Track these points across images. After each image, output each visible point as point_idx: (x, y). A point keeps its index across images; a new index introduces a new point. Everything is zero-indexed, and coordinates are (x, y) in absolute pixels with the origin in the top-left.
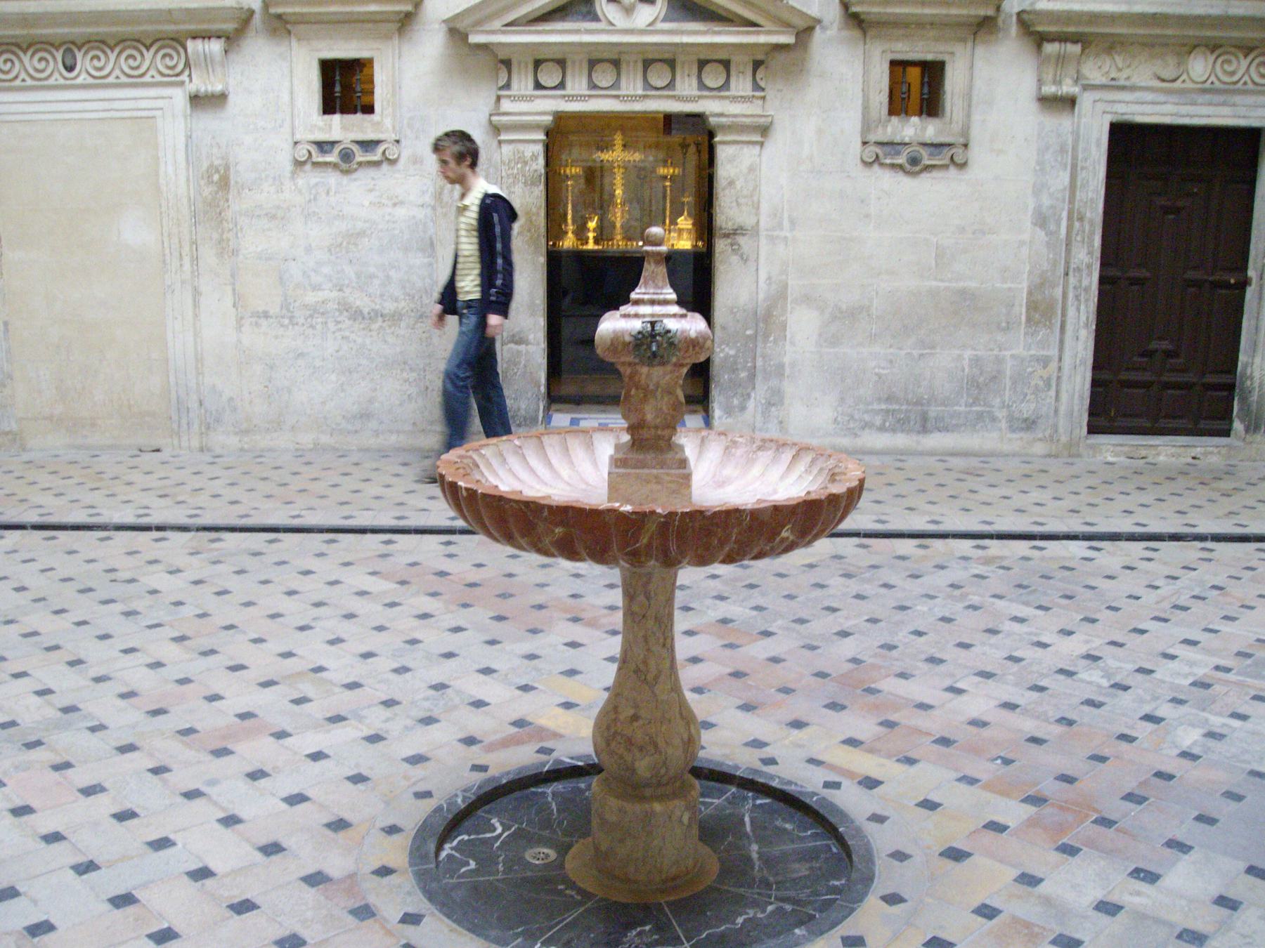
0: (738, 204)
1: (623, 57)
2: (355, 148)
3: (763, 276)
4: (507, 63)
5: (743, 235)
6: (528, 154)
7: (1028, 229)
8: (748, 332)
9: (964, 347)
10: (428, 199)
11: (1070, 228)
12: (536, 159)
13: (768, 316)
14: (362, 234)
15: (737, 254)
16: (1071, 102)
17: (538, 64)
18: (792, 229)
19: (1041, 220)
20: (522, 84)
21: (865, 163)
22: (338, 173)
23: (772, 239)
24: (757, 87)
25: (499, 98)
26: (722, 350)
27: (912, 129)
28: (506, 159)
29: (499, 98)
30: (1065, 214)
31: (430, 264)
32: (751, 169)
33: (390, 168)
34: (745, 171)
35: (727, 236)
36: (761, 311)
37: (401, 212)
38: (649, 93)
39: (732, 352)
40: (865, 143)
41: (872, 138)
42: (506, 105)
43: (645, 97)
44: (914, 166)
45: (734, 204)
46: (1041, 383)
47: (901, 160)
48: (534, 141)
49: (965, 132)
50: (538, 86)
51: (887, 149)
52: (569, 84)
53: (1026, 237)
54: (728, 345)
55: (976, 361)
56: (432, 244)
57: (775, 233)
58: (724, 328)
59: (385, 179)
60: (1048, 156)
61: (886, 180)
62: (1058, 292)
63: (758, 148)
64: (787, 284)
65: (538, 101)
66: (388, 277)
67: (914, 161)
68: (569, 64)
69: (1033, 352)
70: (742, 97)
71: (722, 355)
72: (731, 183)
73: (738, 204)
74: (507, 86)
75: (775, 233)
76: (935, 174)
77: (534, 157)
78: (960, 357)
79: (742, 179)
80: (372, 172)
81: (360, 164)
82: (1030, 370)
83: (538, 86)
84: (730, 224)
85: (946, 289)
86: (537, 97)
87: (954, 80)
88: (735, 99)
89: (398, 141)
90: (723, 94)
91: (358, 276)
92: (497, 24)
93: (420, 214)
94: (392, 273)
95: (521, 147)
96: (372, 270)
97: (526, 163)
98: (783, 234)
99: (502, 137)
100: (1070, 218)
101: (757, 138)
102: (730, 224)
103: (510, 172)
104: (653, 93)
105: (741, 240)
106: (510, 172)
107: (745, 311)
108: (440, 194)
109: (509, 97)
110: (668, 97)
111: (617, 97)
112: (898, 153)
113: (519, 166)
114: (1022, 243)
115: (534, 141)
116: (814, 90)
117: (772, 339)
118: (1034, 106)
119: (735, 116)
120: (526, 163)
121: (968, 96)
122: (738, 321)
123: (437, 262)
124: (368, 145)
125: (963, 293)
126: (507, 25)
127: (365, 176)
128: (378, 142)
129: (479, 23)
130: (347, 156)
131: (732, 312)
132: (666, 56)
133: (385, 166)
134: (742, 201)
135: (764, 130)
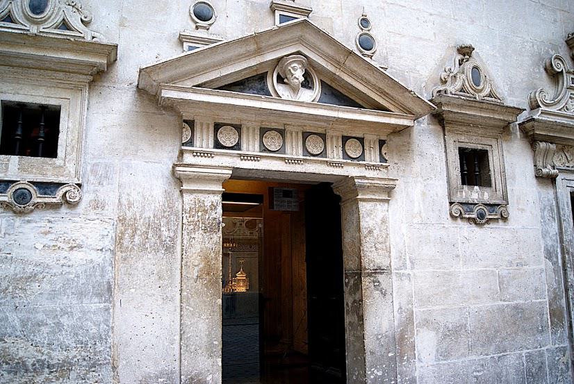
0: (376, 249)
1: (288, 128)
2: (32, 189)
3: (396, 307)
4: (191, 124)
5: (381, 273)
6: (208, 204)
7: (545, 264)
8: (390, 355)
9: (521, 348)
10: (108, 243)
11: (563, 258)
12: (215, 208)
13: (402, 338)
14: (32, 278)
15: (378, 290)
16: (552, 180)
17: (217, 127)
18: (412, 268)
19: (549, 255)
20: (204, 141)
21: (452, 216)
22: (11, 214)
23: (400, 276)
24: (383, 159)
25: (182, 153)
26: (373, 372)
27: (475, 194)
28: (187, 207)
29: (182, 153)
30: (559, 250)
31: (107, 310)
32: (384, 221)
33: (68, 211)
34: (380, 222)
35: (370, 275)
36: (397, 337)
37: (77, 256)
38: (308, 158)
39: (380, 374)
40: (451, 203)
41: (456, 199)
42: (188, 159)
43: (305, 160)
44: (479, 221)
45: (374, 249)
46: (563, 367)
47: (474, 216)
48: (214, 192)
49: (505, 197)
50: (218, 145)
51: (465, 207)
52: (244, 146)
53: (543, 267)
54: (376, 368)
55: (529, 356)
56: (109, 289)
57: (402, 272)
58: (372, 353)
59: (65, 224)
60: (546, 213)
61: (466, 229)
62: (564, 301)
63: (386, 204)
64: (413, 312)
65: (217, 158)
66: (59, 324)
67: (481, 216)
68: (244, 129)
69: (557, 346)
70: (373, 166)
71: (372, 377)
72: (370, 232)
73: (376, 249)
74: (191, 143)
75: (402, 272)
76: (492, 225)
77: (213, 207)
78: (520, 356)
79: (378, 229)
80: (49, 215)
81: (37, 206)
82: (557, 358)
83: (218, 145)
84: (372, 265)
85: (508, 306)
86: (217, 154)
87: (494, 161)
88: (368, 167)
89: (79, 185)
90: (361, 162)
91: (24, 323)
92: (189, 84)
93: (97, 257)
94: (65, 320)
95: (201, 197)
96: (41, 316)
97: (206, 212)
98: (406, 272)
99: (185, 187)
100: (563, 253)
101: (384, 197)
102: (372, 265)
103: (191, 219)
104: (312, 158)
105: (380, 278)
106: (191, 219)
107: (386, 336)
108: (121, 238)
109: (192, 152)
110: (321, 162)
111: (283, 159)
112: (472, 211)
113: (200, 214)
114: (542, 271)
115: (214, 192)
116: (418, 165)
117: (405, 358)
118: (534, 181)
119: (373, 179)
120: (206, 212)
121: (503, 172)
122: (382, 345)
123: (114, 306)
124: (47, 187)
125: (516, 307)
126: (198, 86)
127: (40, 220)
128: (60, 185)
129: (173, 80)
130: (22, 197)
131: (378, 339)
132: (320, 131)
133: (64, 210)
134: (378, 246)
135: (389, 190)
